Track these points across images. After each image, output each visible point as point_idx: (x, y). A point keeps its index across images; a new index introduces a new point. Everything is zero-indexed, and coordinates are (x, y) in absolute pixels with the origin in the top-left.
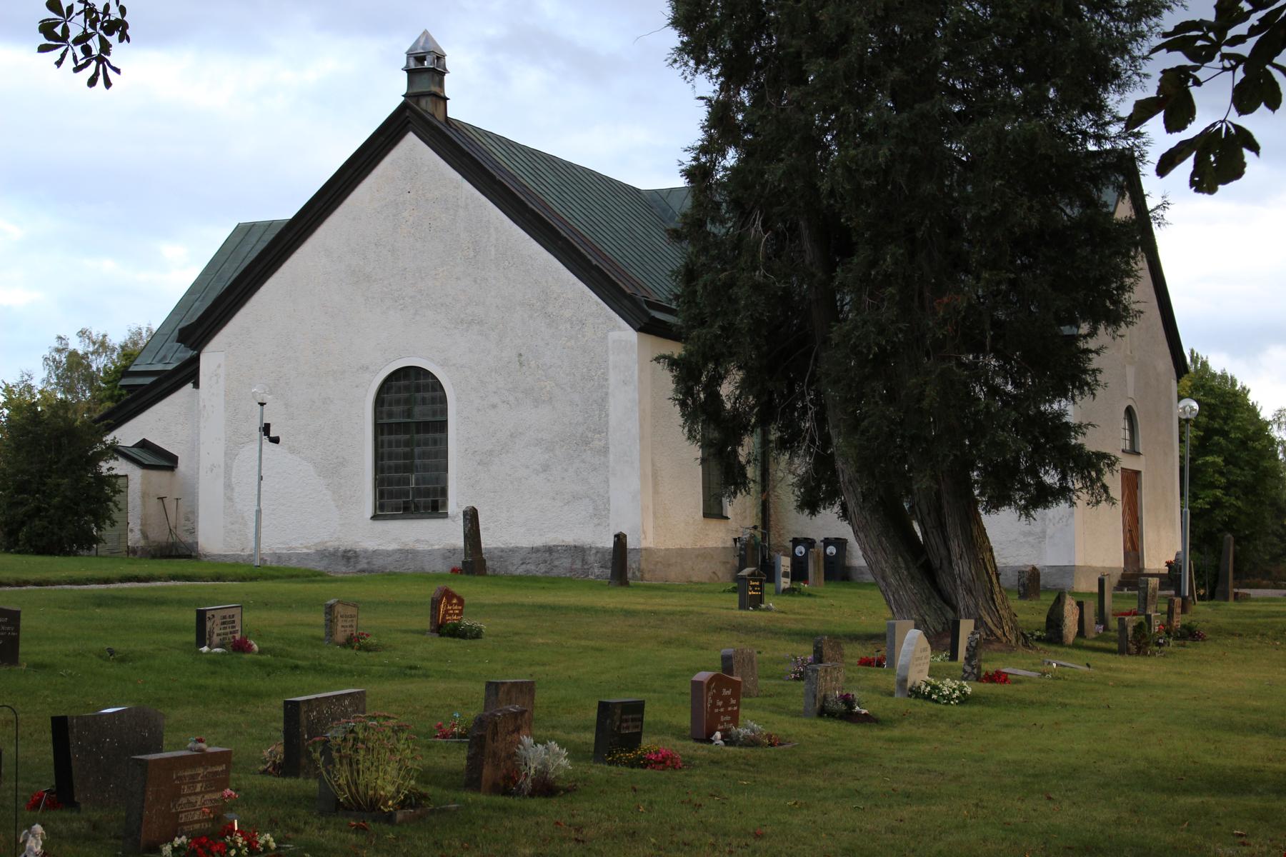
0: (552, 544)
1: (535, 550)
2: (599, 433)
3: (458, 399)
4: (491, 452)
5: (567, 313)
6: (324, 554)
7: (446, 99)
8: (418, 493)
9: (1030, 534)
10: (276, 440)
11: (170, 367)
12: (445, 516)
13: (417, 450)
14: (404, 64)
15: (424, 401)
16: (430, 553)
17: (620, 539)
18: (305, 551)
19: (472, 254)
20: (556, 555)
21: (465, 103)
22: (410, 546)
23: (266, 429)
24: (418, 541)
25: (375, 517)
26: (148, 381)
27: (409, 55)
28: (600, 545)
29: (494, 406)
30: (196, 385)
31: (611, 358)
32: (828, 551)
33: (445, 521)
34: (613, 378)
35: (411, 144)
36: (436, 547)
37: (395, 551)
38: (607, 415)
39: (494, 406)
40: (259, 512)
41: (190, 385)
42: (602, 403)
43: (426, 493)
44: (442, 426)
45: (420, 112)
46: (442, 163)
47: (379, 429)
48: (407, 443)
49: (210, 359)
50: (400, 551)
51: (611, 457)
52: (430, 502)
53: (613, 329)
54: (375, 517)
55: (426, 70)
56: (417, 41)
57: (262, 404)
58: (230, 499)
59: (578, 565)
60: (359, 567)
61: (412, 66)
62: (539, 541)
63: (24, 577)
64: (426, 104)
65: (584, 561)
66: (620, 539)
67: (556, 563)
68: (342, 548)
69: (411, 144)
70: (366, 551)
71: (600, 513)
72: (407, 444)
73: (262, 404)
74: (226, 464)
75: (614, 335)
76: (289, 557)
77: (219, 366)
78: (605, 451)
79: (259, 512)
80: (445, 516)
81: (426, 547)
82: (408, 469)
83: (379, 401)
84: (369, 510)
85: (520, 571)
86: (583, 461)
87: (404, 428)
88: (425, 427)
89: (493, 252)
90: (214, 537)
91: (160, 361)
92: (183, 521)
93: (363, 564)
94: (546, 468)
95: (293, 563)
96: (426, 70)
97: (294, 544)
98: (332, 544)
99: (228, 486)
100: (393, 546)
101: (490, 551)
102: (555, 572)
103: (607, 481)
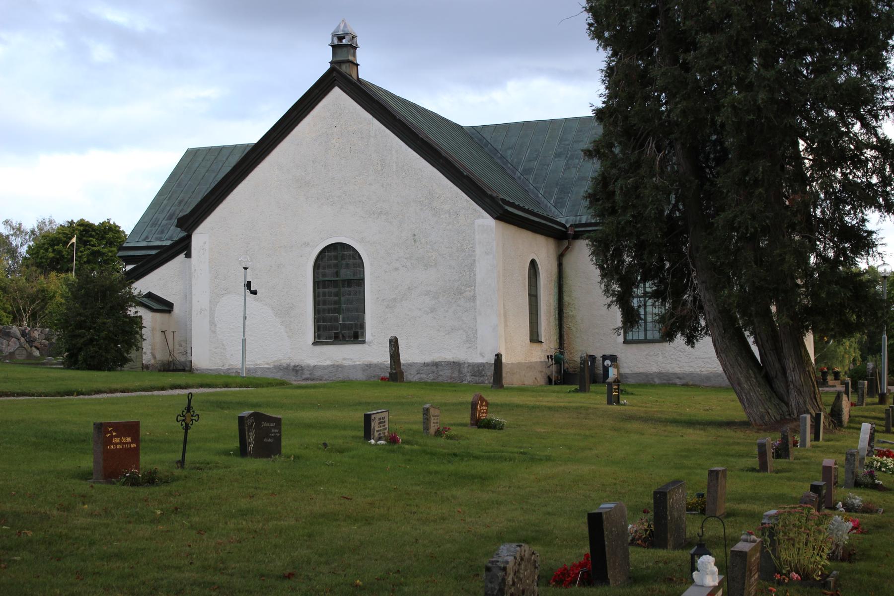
0: (438, 360)
1: (426, 365)
2: (470, 287)
3: (371, 265)
4: (395, 299)
5: (446, 207)
6: (279, 368)
7: (357, 65)
8: (344, 327)
10: (254, 293)
11: (168, 243)
12: (364, 342)
14: (330, 42)
15: (347, 266)
16: (354, 367)
17: (498, 357)
18: (267, 366)
19: (380, 168)
20: (440, 368)
21: (371, 69)
22: (340, 362)
23: (248, 285)
24: (344, 359)
25: (315, 343)
26: (153, 252)
27: (333, 36)
28: (470, 361)
29: (397, 269)
30: (188, 255)
31: (477, 237)
32: (606, 363)
34: (479, 251)
35: (337, 94)
36: (358, 363)
37: (328, 366)
38: (475, 275)
39: (397, 269)
40: (244, 341)
41: (182, 256)
43: (349, 327)
44: (361, 282)
45: (341, 76)
46: (359, 107)
47: (317, 284)
49: (199, 238)
50: (333, 366)
51: (478, 302)
52: (354, 333)
53: (478, 217)
54: (315, 343)
55: (344, 47)
56: (339, 26)
57: (246, 268)
58: (214, 332)
59: (456, 375)
60: (304, 377)
61: (336, 42)
62: (428, 359)
63: (114, 386)
64: (344, 68)
65: (460, 372)
66: (498, 357)
67: (441, 373)
68: (292, 364)
69: (337, 94)
70: (309, 366)
71: (471, 340)
72: (336, 294)
73: (246, 268)
74: (211, 309)
75: (479, 222)
76: (256, 370)
77: (205, 243)
78: (473, 298)
79: (244, 341)
80: (364, 342)
81: (351, 363)
82: (338, 311)
83: (316, 266)
84: (311, 338)
85: (416, 378)
86: (458, 305)
87: (335, 283)
88: (349, 283)
89: (394, 167)
90: (203, 357)
91: (144, 240)
92: (177, 347)
93: (307, 375)
94: (433, 310)
95: (259, 374)
96: (344, 47)
97: (259, 362)
98: (285, 361)
99: (212, 323)
100: (328, 363)
101: (411, 365)
102: (440, 379)
103: (475, 319)
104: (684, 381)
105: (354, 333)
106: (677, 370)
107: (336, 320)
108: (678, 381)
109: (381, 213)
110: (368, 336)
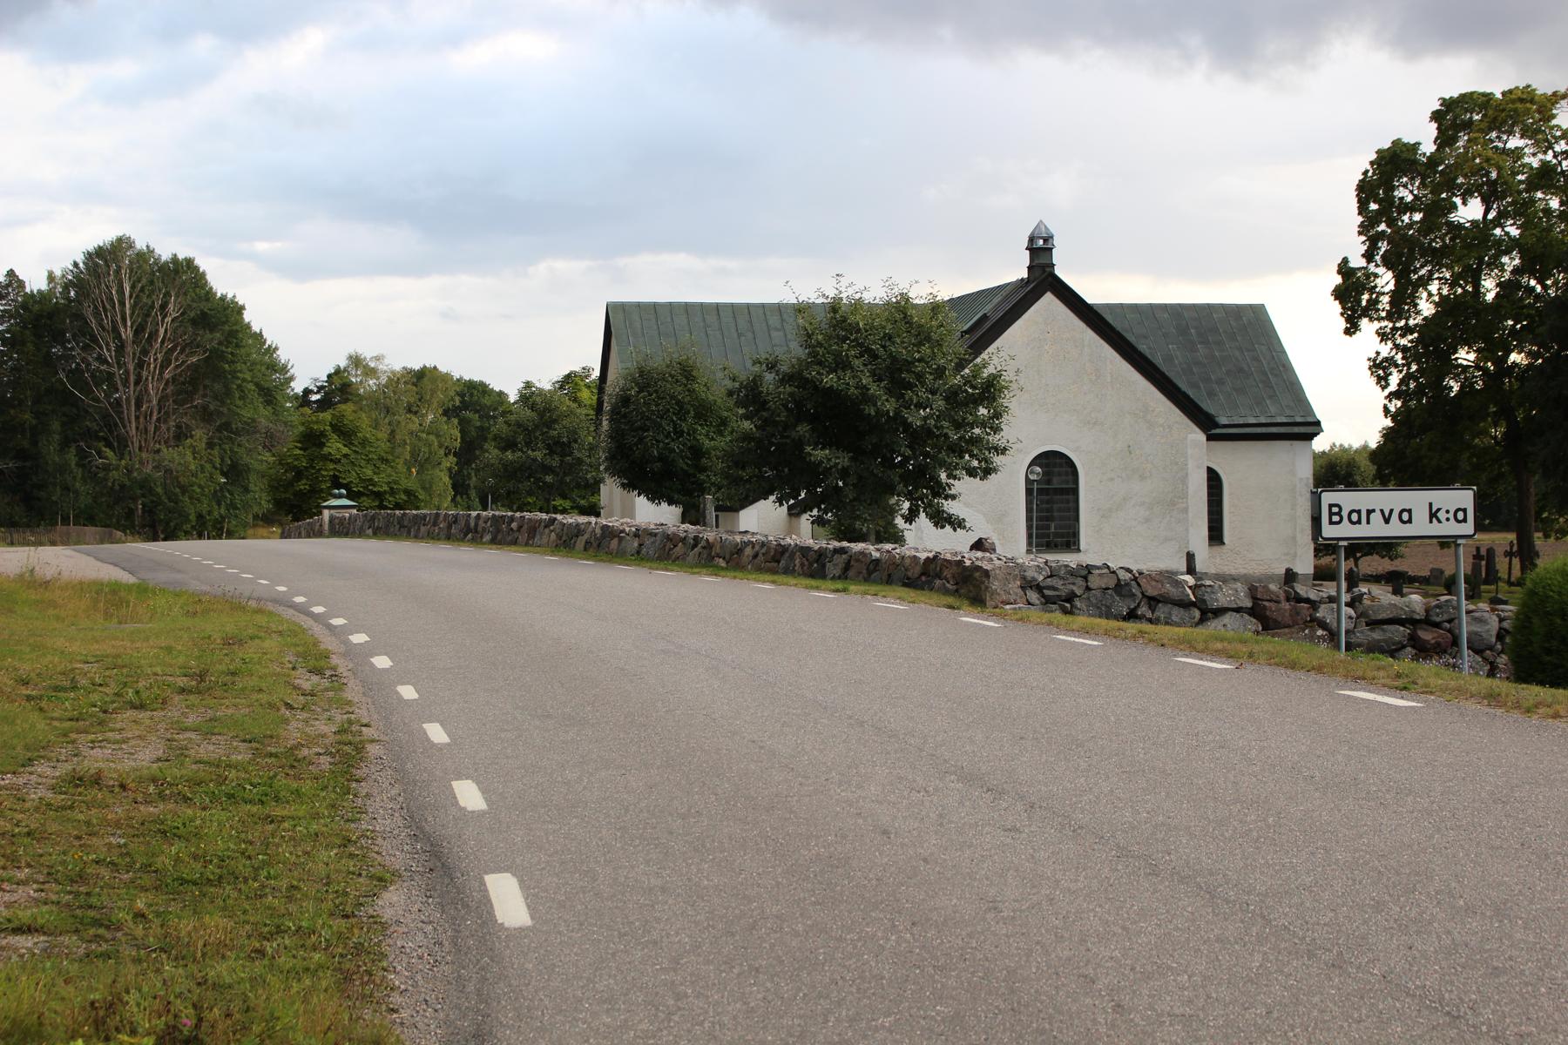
5: (1161, 421)
8: (1056, 535)
12: (1079, 550)
13: (1055, 506)
15: (1060, 474)
31: (1190, 451)
35: (1049, 299)
43: (1062, 536)
44: (1075, 491)
45: (1042, 278)
48: (1048, 502)
55: (1040, 250)
69: (1049, 299)
72: (1048, 502)
75: (1191, 436)
78: (1186, 510)
88: (1062, 491)
94: (1147, 520)
96: (1040, 250)
105: (1070, 541)
107: (1048, 527)
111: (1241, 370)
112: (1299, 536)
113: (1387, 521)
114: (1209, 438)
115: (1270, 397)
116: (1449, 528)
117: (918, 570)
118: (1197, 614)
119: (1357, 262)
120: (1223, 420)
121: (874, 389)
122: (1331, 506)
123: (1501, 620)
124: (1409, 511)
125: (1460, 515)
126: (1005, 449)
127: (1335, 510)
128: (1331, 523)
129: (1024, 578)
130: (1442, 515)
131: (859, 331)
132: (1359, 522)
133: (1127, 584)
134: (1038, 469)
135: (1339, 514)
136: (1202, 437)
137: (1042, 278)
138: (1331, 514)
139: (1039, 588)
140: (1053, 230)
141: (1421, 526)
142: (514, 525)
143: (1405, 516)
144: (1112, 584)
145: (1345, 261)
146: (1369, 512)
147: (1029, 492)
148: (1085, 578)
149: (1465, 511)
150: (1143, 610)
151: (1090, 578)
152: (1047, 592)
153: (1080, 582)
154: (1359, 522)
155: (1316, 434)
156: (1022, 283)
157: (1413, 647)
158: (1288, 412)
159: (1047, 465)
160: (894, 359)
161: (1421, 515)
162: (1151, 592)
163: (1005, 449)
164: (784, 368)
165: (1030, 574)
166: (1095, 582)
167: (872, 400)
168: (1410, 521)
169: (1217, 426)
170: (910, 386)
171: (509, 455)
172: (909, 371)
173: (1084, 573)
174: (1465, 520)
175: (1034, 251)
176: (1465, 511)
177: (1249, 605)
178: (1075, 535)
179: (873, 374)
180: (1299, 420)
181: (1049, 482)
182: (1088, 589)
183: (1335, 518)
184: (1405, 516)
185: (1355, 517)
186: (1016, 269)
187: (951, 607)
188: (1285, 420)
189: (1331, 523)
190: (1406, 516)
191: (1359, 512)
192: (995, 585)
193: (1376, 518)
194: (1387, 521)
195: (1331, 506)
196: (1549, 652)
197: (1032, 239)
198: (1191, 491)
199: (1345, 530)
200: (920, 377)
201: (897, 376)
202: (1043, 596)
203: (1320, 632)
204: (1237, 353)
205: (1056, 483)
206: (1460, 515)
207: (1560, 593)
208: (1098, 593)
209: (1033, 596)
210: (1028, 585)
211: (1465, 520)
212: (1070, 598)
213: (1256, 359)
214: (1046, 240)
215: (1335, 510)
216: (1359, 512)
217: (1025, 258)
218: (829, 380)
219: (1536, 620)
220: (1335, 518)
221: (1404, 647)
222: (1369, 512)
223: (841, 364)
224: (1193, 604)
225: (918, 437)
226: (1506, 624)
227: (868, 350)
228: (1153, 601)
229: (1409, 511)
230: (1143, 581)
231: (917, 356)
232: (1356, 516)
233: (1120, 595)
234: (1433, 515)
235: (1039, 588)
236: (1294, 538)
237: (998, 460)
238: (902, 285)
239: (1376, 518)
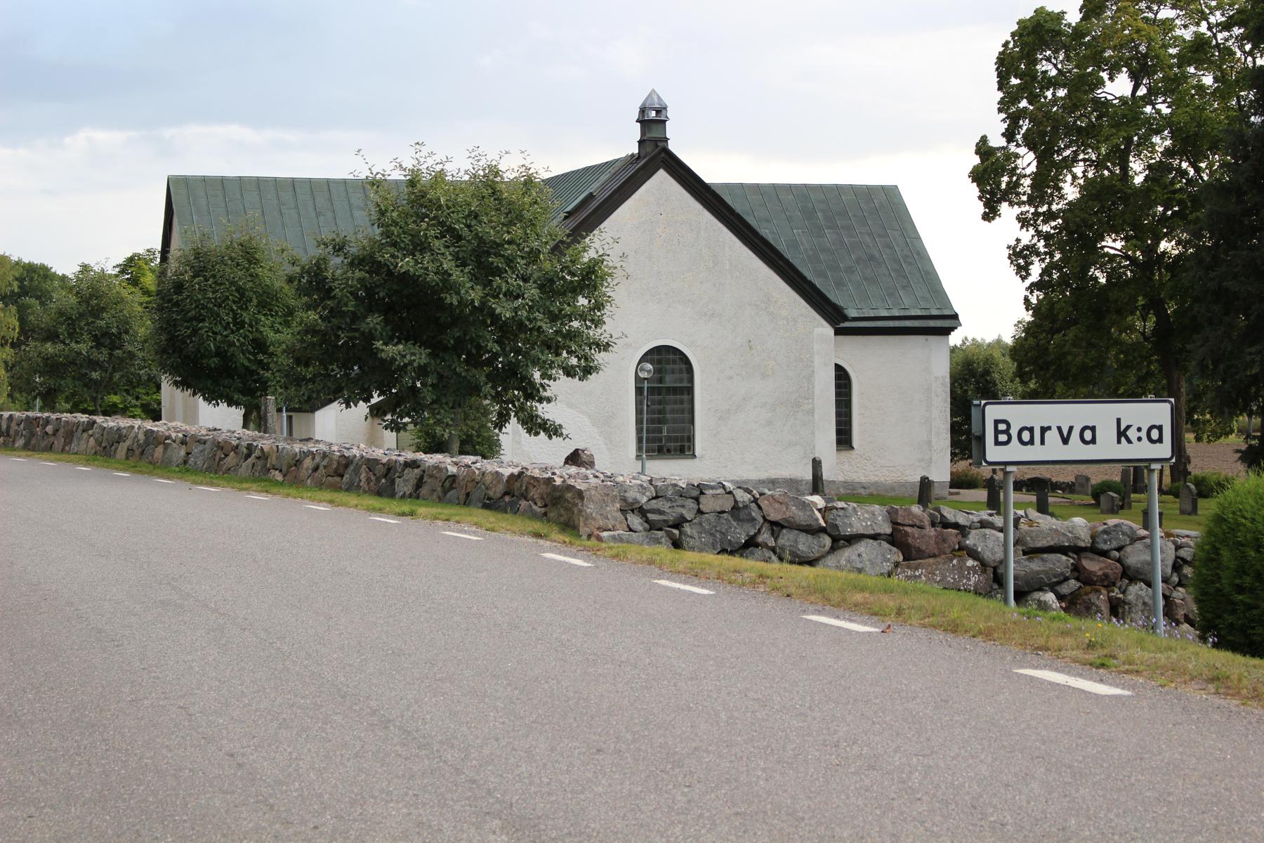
8: (669, 439)
9: (922, 460)
12: (694, 456)
13: (668, 408)
15: (673, 372)
29: (730, 378)
33: (696, 460)
34: (817, 361)
35: (661, 177)
39: (730, 378)
42: (810, 378)
43: (676, 439)
44: (690, 391)
45: (654, 155)
51: (816, 416)
52: (682, 446)
55: (652, 122)
58: (519, 443)
69: (661, 177)
72: (660, 403)
75: (818, 330)
94: (769, 423)
96: (652, 122)
103: (813, 433)
104: (868, 491)
105: (682, 446)
106: (863, 479)
107: (660, 431)
108: (862, 491)
109: (712, 315)
110: (698, 450)
111: (871, 258)
112: (934, 440)
113: (1065, 441)
114: (838, 332)
115: (904, 287)
116: (1141, 450)
117: (500, 489)
118: (827, 541)
119: (997, 141)
120: (852, 313)
121: (457, 275)
122: (997, 422)
123: (1178, 548)
124: (1093, 429)
125: (1155, 434)
126: (608, 345)
127: (1002, 427)
128: (997, 443)
129: (624, 500)
130: (1132, 434)
131: (440, 207)
132: (1031, 442)
133: (746, 507)
134: (649, 366)
135: (1007, 432)
136: (829, 331)
137: (654, 155)
138: (997, 432)
139: (642, 512)
140: (667, 101)
141: (1107, 447)
142: (49, 429)
143: (1088, 435)
144: (728, 507)
145: (984, 139)
146: (1044, 430)
147: (639, 391)
148: (697, 499)
149: (1160, 428)
150: (765, 537)
151: (702, 499)
152: (651, 516)
153: (691, 504)
154: (1031, 442)
155: (953, 329)
156: (633, 159)
157: (1077, 579)
158: (923, 305)
159: (659, 362)
160: (481, 240)
161: (1107, 434)
162: (773, 516)
163: (608, 345)
164: (353, 250)
165: (631, 495)
166: (707, 504)
167: (454, 288)
168: (1093, 441)
169: (846, 318)
170: (499, 272)
171: (49, 348)
172: (498, 255)
173: (695, 493)
174: (1160, 440)
175: (644, 123)
176: (1160, 428)
177: (889, 531)
178: (690, 439)
179: (456, 257)
180: (935, 312)
181: (661, 380)
182: (700, 512)
183: (1003, 438)
184: (1088, 435)
185: (1026, 436)
186: (626, 143)
187: (538, 535)
188: (919, 313)
189: (997, 443)
190: (1089, 435)
191: (1031, 430)
192: (590, 508)
193: (1052, 436)
194: (1065, 441)
195: (997, 422)
196: (1240, 589)
197: (643, 111)
198: (817, 391)
199: (1014, 452)
200: (510, 261)
201: (483, 260)
202: (647, 521)
203: (970, 563)
204: (868, 239)
205: (669, 381)
206: (1155, 434)
207: (1253, 520)
208: (712, 517)
209: (635, 521)
210: (632, 507)
211: (1160, 440)
212: (679, 524)
213: (890, 247)
214: (658, 112)
215: (1002, 427)
216: (1031, 430)
217: (636, 132)
218: (405, 264)
219: (1225, 553)
220: (1003, 438)
221: (1066, 579)
222: (1044, 430)
223: (419, 246)
224: (823, 530)
225: (509, 331)
226: (1182, 553)
227: (451, 230)
228: (776, 527)
229: (1093, 429)
230: (764, 503)
231: (507, 237)
232: (1029, 436)
233: (738, 519)
234: (1122, 434)
235: (642, 512)
236: (929, 442)
237: (600, 357)
238: (492, 157)
239: (1052, 436)
